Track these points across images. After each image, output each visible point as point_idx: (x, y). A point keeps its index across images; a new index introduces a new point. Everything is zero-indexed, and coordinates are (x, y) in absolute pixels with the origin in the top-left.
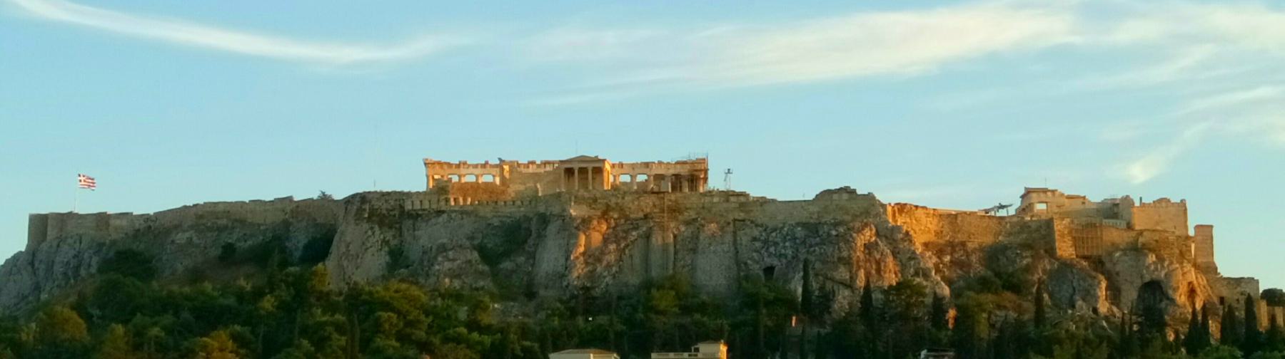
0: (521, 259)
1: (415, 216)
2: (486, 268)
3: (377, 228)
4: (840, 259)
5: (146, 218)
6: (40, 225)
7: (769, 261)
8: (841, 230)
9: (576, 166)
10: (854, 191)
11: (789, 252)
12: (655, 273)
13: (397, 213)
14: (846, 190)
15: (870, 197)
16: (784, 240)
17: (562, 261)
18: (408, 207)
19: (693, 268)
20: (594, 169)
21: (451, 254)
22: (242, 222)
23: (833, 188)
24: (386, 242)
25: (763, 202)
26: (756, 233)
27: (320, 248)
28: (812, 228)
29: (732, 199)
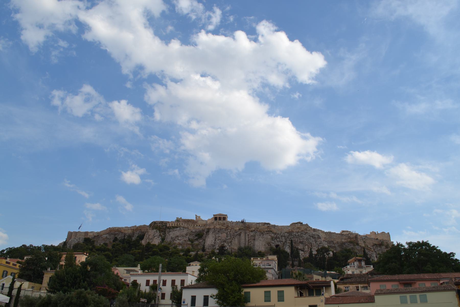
0: (201, 241)
1: (169, 228)
2: (190, 243)
3: (158, 231)
4: (300, 242)
5: (97, 233)
6: (70, 235)
7: (277, 243)
8: (299, 234)
10: (302, 223)
11: (284, 240)
12: (242, 246)
14: (300, 223)
16: (282, 237)
18: (168, 225)
19: (254, 245)
20: (223, 218)
21: (180, 238)
22: (121, 232)
25: (274, 226)
27: (141, 237)
28: (290, 233)
29: (266, 225)
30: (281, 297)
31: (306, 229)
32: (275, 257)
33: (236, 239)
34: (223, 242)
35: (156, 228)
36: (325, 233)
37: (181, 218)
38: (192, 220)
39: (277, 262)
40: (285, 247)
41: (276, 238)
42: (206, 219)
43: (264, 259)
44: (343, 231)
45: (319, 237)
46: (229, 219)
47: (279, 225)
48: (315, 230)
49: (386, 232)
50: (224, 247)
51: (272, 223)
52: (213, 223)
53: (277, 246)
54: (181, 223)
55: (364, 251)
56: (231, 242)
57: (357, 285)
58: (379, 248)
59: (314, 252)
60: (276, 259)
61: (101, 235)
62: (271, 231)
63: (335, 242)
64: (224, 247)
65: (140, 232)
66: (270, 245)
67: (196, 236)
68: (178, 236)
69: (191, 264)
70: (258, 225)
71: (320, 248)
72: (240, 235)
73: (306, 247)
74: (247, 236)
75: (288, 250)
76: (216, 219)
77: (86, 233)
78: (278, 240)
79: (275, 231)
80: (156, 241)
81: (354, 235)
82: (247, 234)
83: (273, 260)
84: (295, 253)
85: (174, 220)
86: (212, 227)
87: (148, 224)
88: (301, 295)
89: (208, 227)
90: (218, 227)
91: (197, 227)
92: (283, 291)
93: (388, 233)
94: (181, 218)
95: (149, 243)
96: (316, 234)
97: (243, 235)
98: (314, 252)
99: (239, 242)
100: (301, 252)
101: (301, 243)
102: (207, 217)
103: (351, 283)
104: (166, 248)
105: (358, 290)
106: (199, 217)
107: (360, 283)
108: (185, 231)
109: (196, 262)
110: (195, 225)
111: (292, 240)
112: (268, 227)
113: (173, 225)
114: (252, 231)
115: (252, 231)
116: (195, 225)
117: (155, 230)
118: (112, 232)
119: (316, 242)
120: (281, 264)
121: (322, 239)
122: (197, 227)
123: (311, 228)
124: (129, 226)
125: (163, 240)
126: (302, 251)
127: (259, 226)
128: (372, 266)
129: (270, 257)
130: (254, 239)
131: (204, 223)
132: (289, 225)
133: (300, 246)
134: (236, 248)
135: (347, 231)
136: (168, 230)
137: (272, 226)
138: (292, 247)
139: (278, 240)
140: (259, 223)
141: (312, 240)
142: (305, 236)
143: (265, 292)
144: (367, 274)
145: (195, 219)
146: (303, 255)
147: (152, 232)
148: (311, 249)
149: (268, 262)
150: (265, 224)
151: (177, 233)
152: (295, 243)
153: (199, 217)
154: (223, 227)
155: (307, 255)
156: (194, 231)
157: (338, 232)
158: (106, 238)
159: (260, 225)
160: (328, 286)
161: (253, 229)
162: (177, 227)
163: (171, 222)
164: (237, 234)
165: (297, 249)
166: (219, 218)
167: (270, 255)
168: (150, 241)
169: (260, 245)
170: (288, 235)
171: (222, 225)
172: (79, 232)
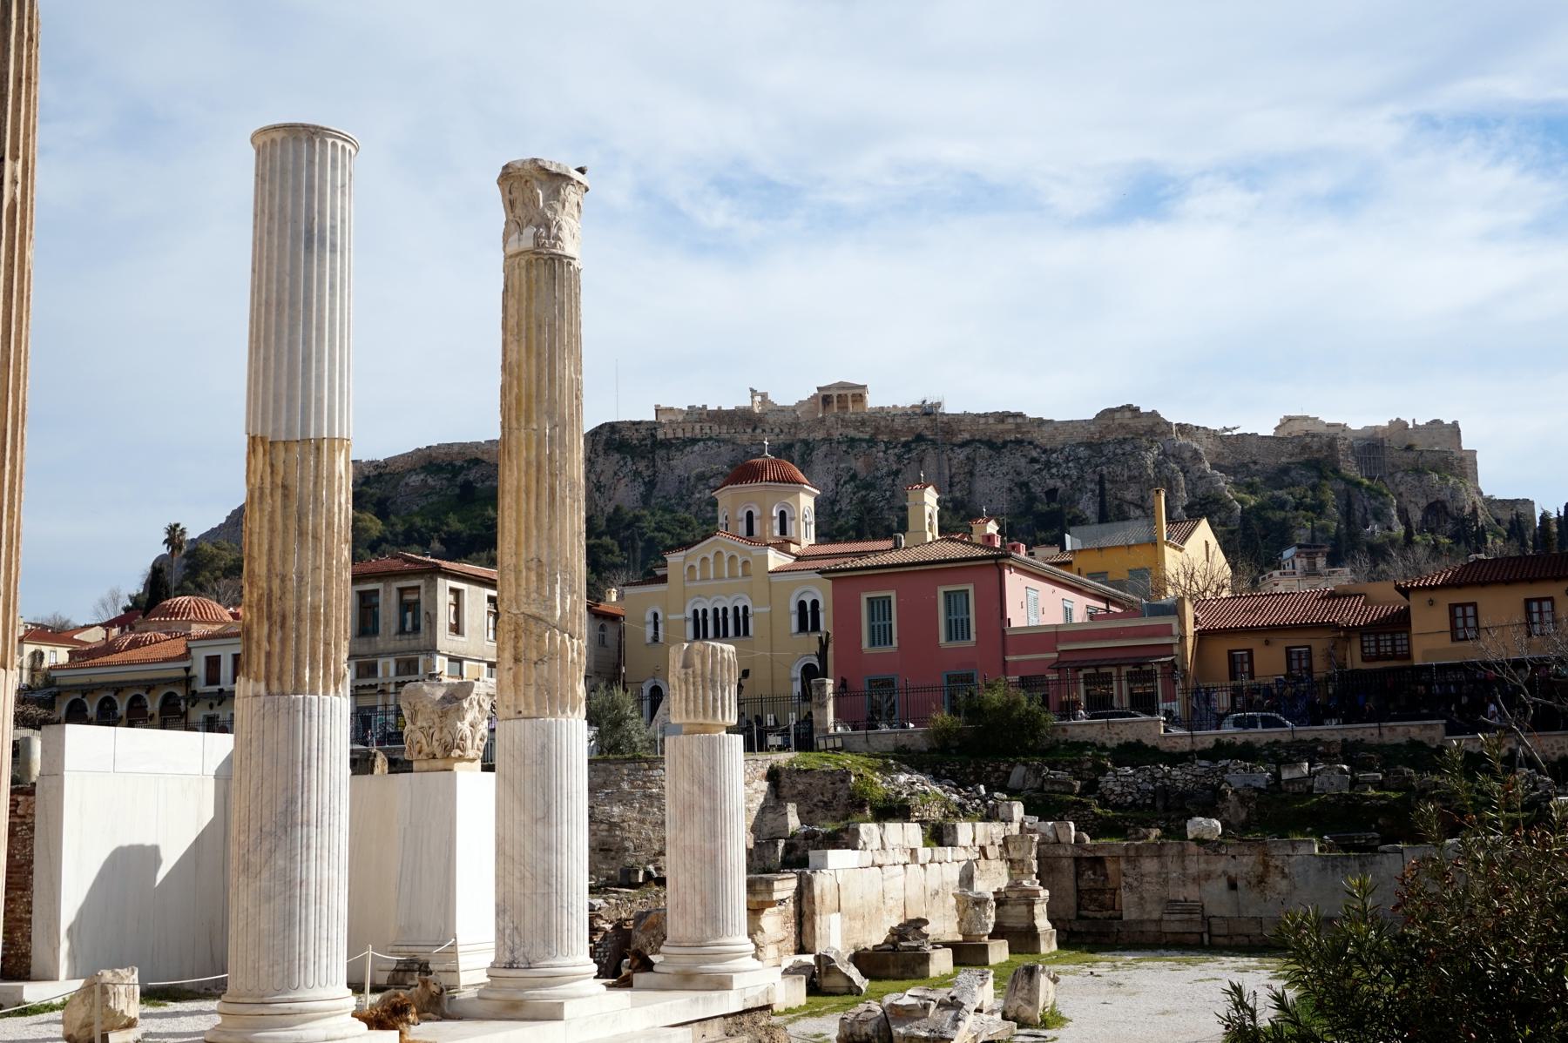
1: (667, 444)
7: (1051, 483)
9: (835, 393)
10: (1137, 409)
15: (1154, 414)
17: (832, 485)
18: (660, 435)
25: (1041, 422)
26: (1035, 454)
28: (1094, 446)
29: (1010, 420)
37: (705, 407)
70: (982, 421)
79: (1040, 437)
94: (705, 407)
112: (1018, 426)
113: (680, 435)
123: (1169, 424)
132: (1092, 416)
152: (1112, 482)
161: (967, 436)
170: (1087, 453)
171: (857, 429)
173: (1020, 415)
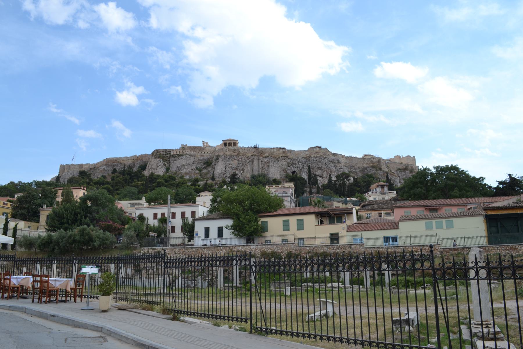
0: (210, 169)
1: (174, 156)
2: (198, 172)
3: (162, 160)
4: (318, 168)
5: (93, 165)
6: (63, 168)
7: (294, 170)
8: (318, 159)
10: (320, 148)
11: (301, 166)
12: (256, 173)
13: (168, 155)
15: (326, 149)
17: (224, 169)
18: (172, 154)
20: (234, 143)
21: (186, 167)
22: (119, 162)
23: (313, 146)
24: (164, 164)
27: (143, 167)
28: (308, 158)
29: (281, 150)
30: (300, 226)
31: (325, 154)
32: (292, 185)
33: (249, 166)
34: (235, 170)
35: (159, 158)
36: (346, 157)
37: (186, 145)
38: (199, 147)
39: (294, 190)
40: (302, 173)
41: (292, 164)
42: (215, 145)
43: (280, 186)
44: (365, 156)
45: (339, 162)
46: (240, 145)
47: (296, 150)
48: (334, 154)
49: (412, 156)
50: (236, 175)
51: (288, 148)
52: (222, 149)
53: (293, 172)
54: (187, 150)
55: (387, 177)
56: (243, 170)
57: (379, 212)
58: (403, 173)
59: (334, 179)
60: (293, 186)
61: (98, 168)
62: (287, 157)
63: (356, 167)
64: (236, 175)
65: (142, 162)
66: (286, 172)
67: (204, 164)
68: (184, 165)
69: (201, 194)
71: (340, 173)
72: (252, 161)
73: (325, 173)
74: (260, 163)
75: (305, 177)
76: (225, 144)
77: (81, 165)
78: (294, 166)
80: (160, 171)
81: (377, 160)
82: (260, 161)
83: (289, 188)
84: (313, 180)
85: (178, 147)
86: (222, 154)
87: (150, 153)
88: (322, 223)
89: (217, 154)
90: (228, 153)
91: (205, 155)
92: (302, 220)
93: (414, 157)
94: (186, 145)
95: (152, 174)
96: (335, 159)
97: (256, 161)
98: (334, 179)
99: (252, 170)
100: (319, 179)
101: (320, 168)
102: (215, 142)
103: (374, 210)
104: (172, 178)
105: (380, 216)
106: (207, 143)
107: (383, 209)
108: (192, 160)
109: (206, 192)
110: (203, 153)
111: (309, 166)
112: (284, 152)
113: (178, 153)
114: (266, 157)
115: (266, 157)
116: (203, 153)
117: (158, 159)
118: (110, 163)
119: (336, 167)
120: (298, 192)
121: (343, 164)
122: (205, 155)
123: (331, 152)
124: (129, 155)
125: (168, 169)
126: (320, 177)
127: (274, 151)
128: (395, 192)
129: (287, 185)
130: (268, 166)
131: (213, 149)
132: (307, 149)
133: (319, 172)
134: (249, 176)
135: (370, 155)
136: (173, 158)
137: (288, 151)
138: (309, 173)
139: (294, 166)
140: (273, 149)
141: (331, 166)
142: (324, 162)
143: (284, 221)
144: (390, 200)
145: (201, 145)
146: (322, 181)
147: (155, 162)
148: (330, 175)
149: (284, 190)
150: (280, 149)
151: (182, 161)
152: (313, 169)
153: (207, 143)
154: (234, 154)
155: (326, 182)
156: (201, 159)
157: (360, 156)
158: (104, 169)
159: (275, 150)
160: (350, 213)
161: (267, 155)
162: (182, 155)
163: (176, 149)
164: (250, 161)
165: (316, 175)
166: (229, 143)
167: (286, 182)
168: (154, 172)
169: (275, 172)
170: (305, 160)
171: (233, 152)
172: (72, 165)
173: (284, 149)
